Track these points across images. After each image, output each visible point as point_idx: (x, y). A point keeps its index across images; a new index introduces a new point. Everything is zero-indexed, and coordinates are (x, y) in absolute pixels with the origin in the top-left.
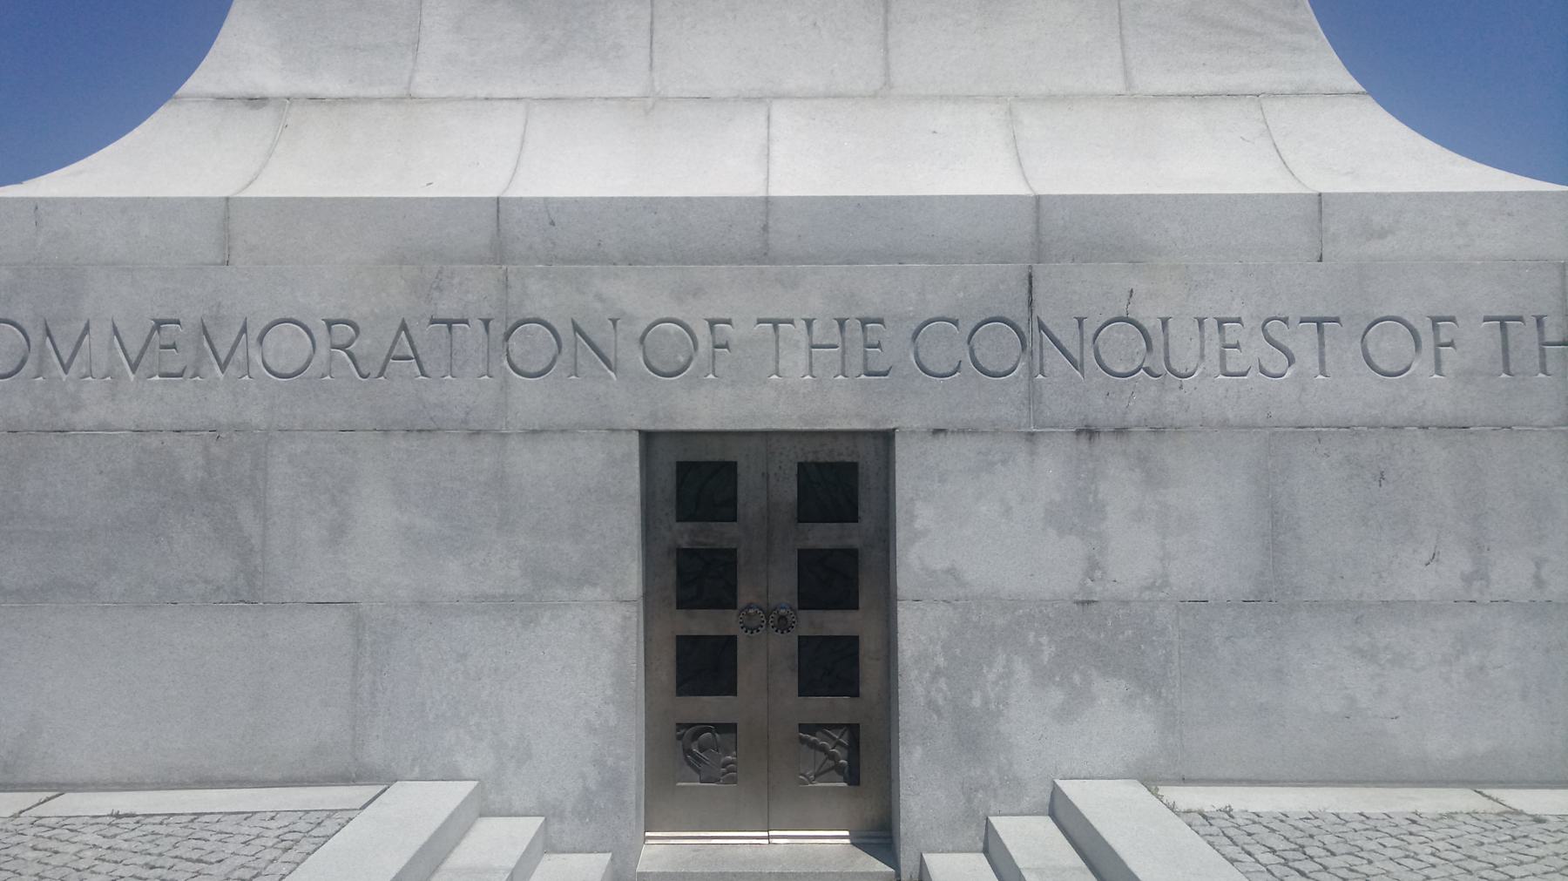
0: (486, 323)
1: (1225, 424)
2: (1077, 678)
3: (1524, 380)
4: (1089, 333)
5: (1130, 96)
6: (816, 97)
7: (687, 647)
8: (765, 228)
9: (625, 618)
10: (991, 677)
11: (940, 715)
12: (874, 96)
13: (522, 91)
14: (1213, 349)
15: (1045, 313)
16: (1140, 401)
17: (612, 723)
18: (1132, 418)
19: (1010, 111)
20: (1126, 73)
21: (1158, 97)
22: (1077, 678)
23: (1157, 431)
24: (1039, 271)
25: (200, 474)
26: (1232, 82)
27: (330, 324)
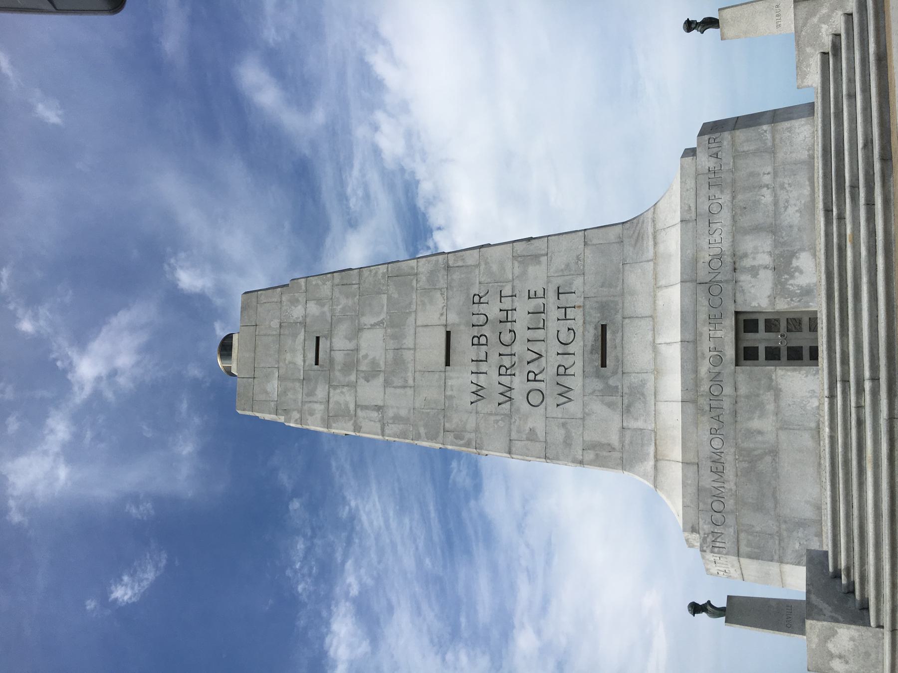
0: (710, 400)
1: (733, 241)
2: (792, 270)
4: (712, 271)
5: (655, 259)
6: (654, 333)
7: (790, 358)
8: (688, 342)
9: (780, 369)
10: (792, 288)
11: (802, 299)
12: (653, 319)
13: (653, 403)
14: (718, 245)
15: (708, 280)
16: (728, 259)
17: (805, 372)
18: (732, 261)
19: (658, 288)
20: (648, 261)
21: (655, 253)
22: (792, 270)
23: (734, 256)
24: (698, 282)
25: (747, 463)
26: (651, 237)
27: (711, 434)
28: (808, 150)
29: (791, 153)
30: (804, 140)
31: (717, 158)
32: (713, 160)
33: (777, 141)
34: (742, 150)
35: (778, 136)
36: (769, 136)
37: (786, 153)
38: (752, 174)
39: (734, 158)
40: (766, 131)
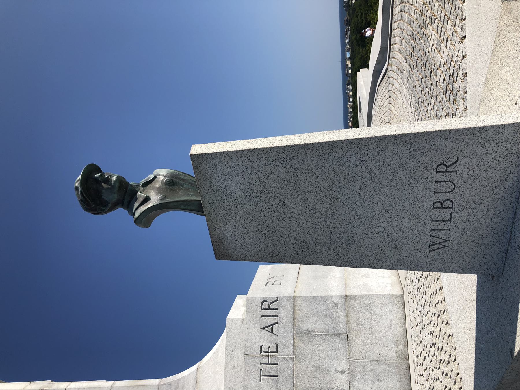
3: (279, 371)
28: (397, 345)
29: (372, 344)
30: (390, 328)
31: (272, 332)
32: (266, 335)
33: (353, 321)
34: (305, 328)
35: (353, 317)
36: (341, 314)
37: (365, 344)
38: (318, 369)
39: (295, 336)
40: (336, 305)
